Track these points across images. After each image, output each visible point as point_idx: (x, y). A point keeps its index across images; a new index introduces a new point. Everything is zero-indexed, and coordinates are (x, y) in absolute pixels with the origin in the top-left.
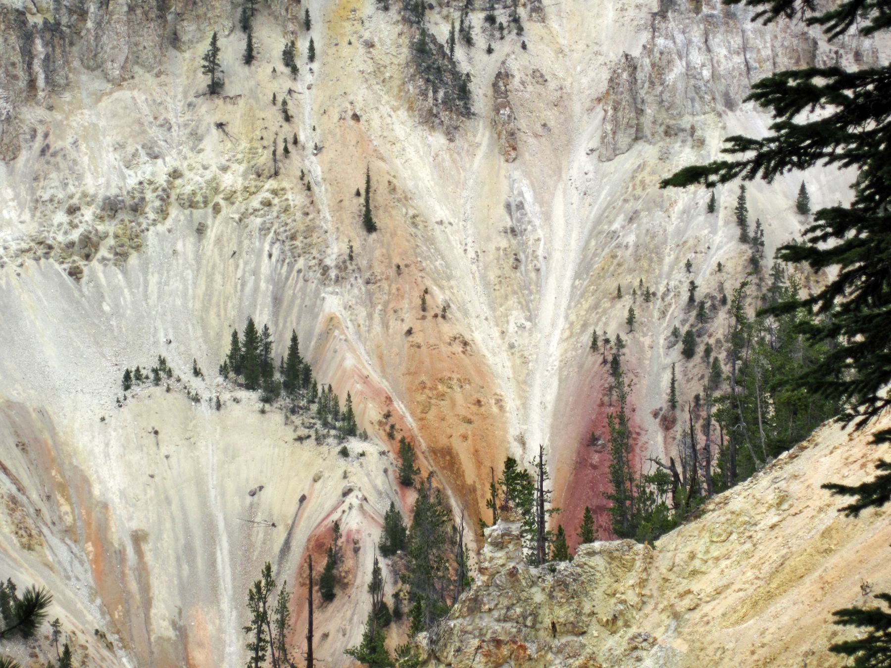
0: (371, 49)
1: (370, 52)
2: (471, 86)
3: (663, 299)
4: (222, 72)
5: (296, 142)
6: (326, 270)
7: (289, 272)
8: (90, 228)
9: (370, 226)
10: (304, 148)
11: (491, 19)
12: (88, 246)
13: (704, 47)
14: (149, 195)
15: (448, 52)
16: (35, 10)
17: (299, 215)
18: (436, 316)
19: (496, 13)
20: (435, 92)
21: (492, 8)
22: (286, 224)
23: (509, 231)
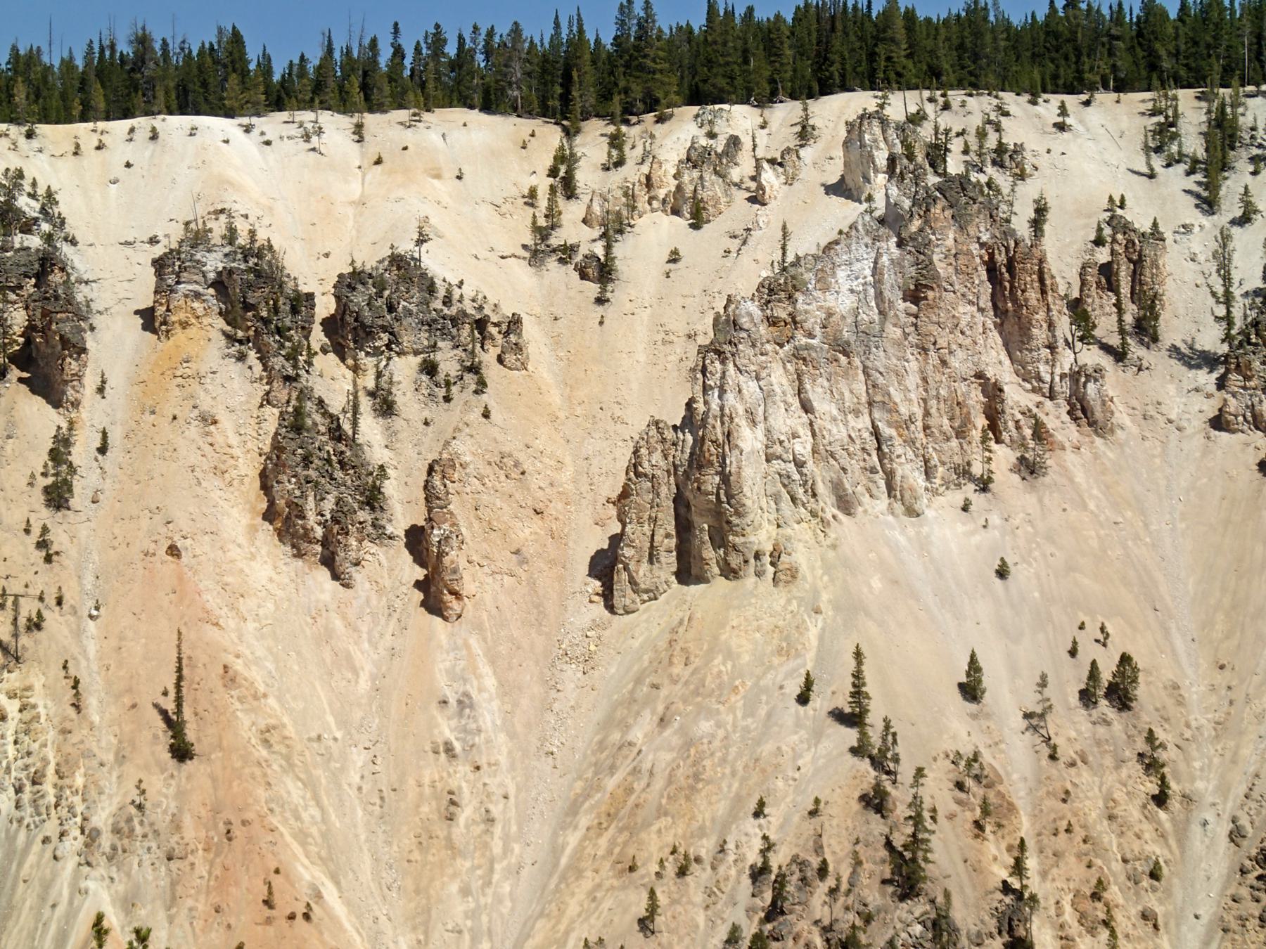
0: (212, 428)
3: (714, 868)
5: (59, 602)
6: (91, 837)
7: (29, 844)
9: (181, 752)
10: (74, 611)
11: (430, 369)
13: (796, 403)
15: (347, 427)
17: (51, 735)
18: (292, 917)
19: (438, 357)
21: (434, 347)
22: (29, 754)
23: (441, 749)
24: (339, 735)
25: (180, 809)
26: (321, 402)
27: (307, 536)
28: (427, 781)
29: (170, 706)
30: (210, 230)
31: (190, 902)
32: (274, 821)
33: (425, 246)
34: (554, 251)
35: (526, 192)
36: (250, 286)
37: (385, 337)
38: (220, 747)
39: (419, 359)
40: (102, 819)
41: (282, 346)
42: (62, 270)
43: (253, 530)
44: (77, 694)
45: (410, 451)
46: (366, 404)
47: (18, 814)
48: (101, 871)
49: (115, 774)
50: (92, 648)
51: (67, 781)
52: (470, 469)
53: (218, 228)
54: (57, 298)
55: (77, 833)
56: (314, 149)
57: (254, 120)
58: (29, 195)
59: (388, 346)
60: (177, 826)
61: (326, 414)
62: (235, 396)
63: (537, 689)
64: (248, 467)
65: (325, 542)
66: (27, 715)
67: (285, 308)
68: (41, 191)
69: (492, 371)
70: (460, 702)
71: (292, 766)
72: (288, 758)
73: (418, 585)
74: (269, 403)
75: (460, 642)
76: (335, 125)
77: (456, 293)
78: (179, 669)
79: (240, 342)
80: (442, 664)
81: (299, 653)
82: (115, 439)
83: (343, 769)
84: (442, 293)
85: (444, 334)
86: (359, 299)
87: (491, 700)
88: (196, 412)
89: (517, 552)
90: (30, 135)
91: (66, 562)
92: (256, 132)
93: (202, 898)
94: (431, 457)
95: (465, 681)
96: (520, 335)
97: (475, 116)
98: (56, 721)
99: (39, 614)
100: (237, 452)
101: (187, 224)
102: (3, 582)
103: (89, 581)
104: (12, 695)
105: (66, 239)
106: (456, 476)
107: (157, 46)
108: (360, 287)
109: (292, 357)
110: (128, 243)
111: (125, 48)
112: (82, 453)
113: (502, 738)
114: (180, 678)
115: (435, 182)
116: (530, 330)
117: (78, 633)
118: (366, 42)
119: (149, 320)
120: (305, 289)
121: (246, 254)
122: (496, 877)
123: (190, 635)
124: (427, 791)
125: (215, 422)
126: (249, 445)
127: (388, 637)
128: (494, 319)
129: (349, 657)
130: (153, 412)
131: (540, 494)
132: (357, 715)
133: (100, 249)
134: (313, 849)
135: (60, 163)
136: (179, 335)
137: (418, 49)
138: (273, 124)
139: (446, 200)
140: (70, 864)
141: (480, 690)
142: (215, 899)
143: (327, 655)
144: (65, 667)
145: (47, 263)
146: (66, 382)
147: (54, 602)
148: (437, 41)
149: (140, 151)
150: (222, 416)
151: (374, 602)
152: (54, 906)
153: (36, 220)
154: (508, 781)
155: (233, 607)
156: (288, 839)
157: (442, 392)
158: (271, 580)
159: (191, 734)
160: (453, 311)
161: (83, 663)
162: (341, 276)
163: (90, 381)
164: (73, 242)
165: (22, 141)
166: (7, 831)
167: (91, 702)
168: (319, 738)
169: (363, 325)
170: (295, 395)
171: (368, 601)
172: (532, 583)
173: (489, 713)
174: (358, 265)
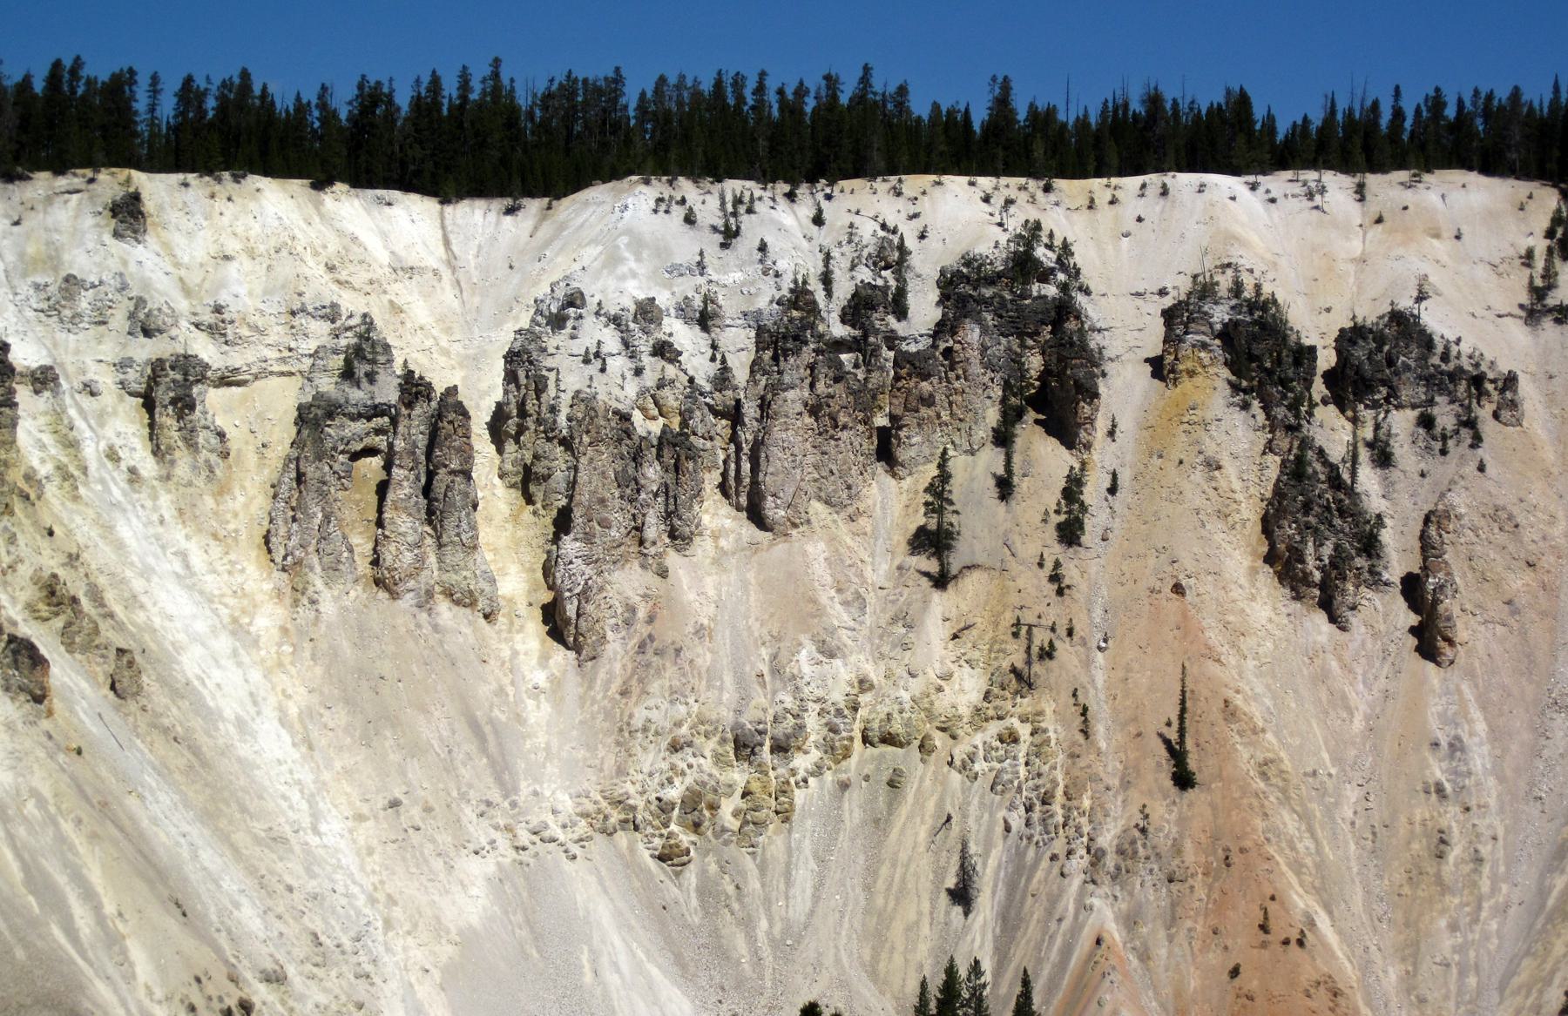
1: (1212, 479)
2: (1386, 536)
4: (957, 512)
5: (1070, 633)
8: (706, 778)
9: (1183, 780)
10: (1084, 643)
11: (1426, 422)
12: (697, 808)
14: (812, 722)
15: (1346, 476)
16: (656, 412)
17: (1061, 758)
18: (1286, 942)
19: (1436, 411)
20: (1319, 545)
21: (1431, 402)
22: (1039, 775)
24: (1333, 771)
25: (1181, 834)
26: (1321, 452)
27: (1306, 579)
28: (1418, 818)
29: (1173, 735)
30: (1217, 284)
31: (1189, 923)
32: (1271, 850)
33: (1424, 304)
34: (1550, 311)
35: (1523, 252)
36: (1254, 338)
37: (1384, 391)
38: (1220, 777)
39: (1416, 413)
40: (1107, 840)
41: (1284, 397)
42: (1078, 318)
43: (1253, 571)
44: (1086, 721)
45: (1405, 501)
46: (1364, 454)
47: (1028, 832)
48: (1105, 889)
49: (1120, 799)
50: (1100, 681)
51: (1075, 803)
52: (1465, 521)
53: (1225, 281)
54: (1072, 344)
55: (1084, 852)
56: (1317, 208)
57: (1260, 178)
58: (1047, 246)
59: (1387, 400)
60: (1177, 850)
61: (1326, 463)
62: (1238, 440)
63: (1526, 736)
64: (1250, 512)
65: (1323, 586)
66: (1038, 739)
67: (1288, 359)
68: (1058, 242)
69: (1488, 427)
70: (1451, 745)
71: (1288, 798)
72: (1284, 791)
73: (1413, 631)
74: (1271, 450)
75: (1452, 687)
76: (1337, 186)
77: (1454, 349)
78: (1183, 702)
79: (1245, 391)
80: (1434, 707)
81: (1295, 691)
82: (1125, 479)
83: (1337, 804)
84: (1439, 349)
85: (1442, 390)
86: (1360, 353)
87: (1481, 744)
88: (1201, 458)
89: (1509, 603)
90: (1047, 189)
91: (1077, 596)
92: (1261, 190)
93: (1201, 920)
94: (1427, 508)
95: (1457, 725)
96: (1515, 392)
97: (1473, 178)
98: (1065, 745)
99: (1051, 644)
100: (1239, 497)
101: (1195, 277)
102: (1018, 612)
103: (1098, 613)
104: (1024, 720)
105: (1080, 289)
106: (1451, 527)
107: (1168, 106)
108: (1361, 342)
109: (1294, 407)
110: (1138, 294)
111: (1136, 106)
112: (1092, 493)
113: (1491, 782)
114: (1183, 710)
115: (1435, 242)
116: (1526, 387)
117: (1088, 663)
118: (1369, 103)
119: (1158, 368)
120: (1307, 342)
121: (1252, 306)
122: (1484, 914)
123: (1193, 670)
124: (1418, 828)
125: (1219, 468)
126: (1252, 490)
127: (1383, 680)
128: (1491, 375)
129: (1344, 697)
130: (1160, 456)
131: (1532, 547)
132: (1353, 752)
133: (1112, 299)
134: (1308, 879)
135: (1075, 216)
136: (1186, 384)
137: (1418, 111)
138: (1278, 182)
139: (1445, 259)
140: (1076, 882)
141: (1471, 734)
142: (1212, 921)
143: (1324, 696)
144: (1074, 695)
145: (1063, 310)
146: (1079, 425)
147: (1064, 633)
148: (1437, 103)
149: (1151, 206)
150: (1226, 461)
151: (1369, 645)
152: (1060, 920)
153: (1053, 270)
154: (1497, 823)
155: (1233, 645)
156: (1284, 868)
157: (1438, 445)
158: (1270, 620)
159: (1192, 763)
160: (1451, 367)
161: (1092, 692)
162: (1342, 331)
163: (1102, 424)
164: (1087, 292)
165: (1040, 194)
166: (1017, 847)
167: (1099, 729)
168: (1314, 773)
169: (1363, 379)
170: (1296, 444)
171: (1363, 643)
172: (1523, 634)
173: (1479, 757)
174: (1359, 320)
